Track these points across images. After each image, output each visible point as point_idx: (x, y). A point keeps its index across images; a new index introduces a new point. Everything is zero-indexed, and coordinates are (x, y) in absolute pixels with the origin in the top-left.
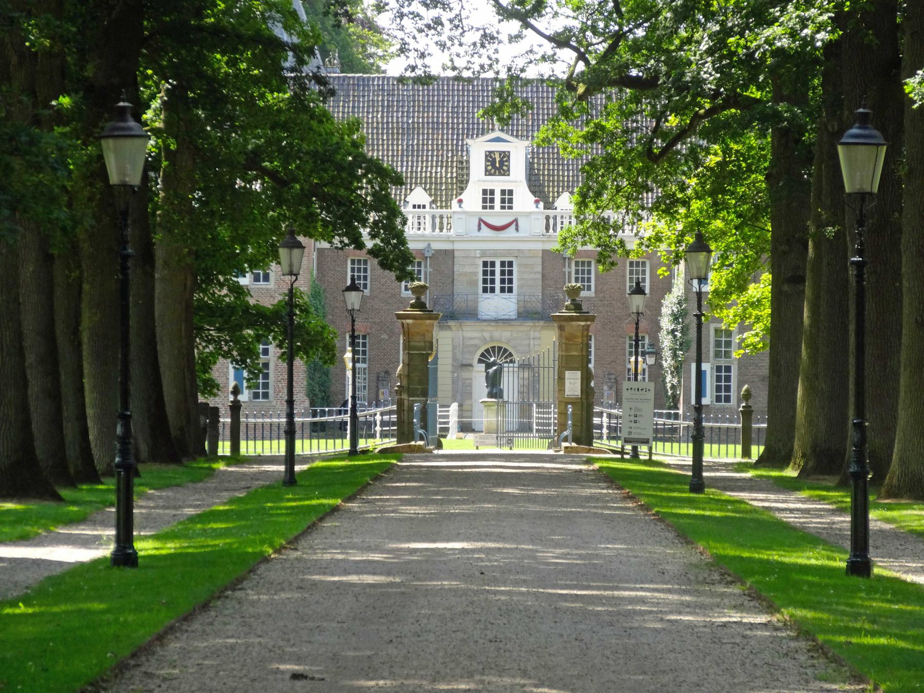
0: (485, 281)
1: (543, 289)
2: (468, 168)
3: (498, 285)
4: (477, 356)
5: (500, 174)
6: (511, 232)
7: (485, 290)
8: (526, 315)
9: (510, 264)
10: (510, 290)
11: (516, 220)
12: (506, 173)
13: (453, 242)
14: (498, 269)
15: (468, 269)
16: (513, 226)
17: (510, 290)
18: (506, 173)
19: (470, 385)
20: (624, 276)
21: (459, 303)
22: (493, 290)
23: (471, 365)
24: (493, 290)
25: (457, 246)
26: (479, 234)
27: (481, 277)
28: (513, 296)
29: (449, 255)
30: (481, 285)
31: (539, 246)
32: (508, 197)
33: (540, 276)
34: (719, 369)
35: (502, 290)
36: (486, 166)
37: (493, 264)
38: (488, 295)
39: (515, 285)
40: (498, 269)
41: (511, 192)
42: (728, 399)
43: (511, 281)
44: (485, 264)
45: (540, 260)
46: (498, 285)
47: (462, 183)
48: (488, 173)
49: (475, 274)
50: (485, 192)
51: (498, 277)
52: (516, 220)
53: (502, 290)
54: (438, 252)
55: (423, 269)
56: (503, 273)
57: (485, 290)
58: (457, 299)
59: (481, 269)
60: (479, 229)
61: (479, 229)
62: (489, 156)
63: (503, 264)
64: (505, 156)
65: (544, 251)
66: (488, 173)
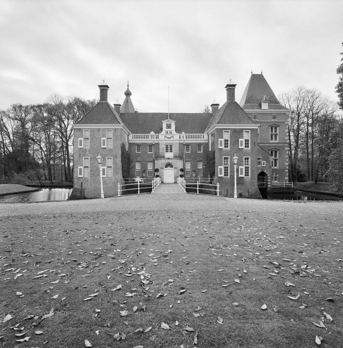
0: (166, 150)
1: (179, 151)
2: (163, 129)
3: (169, 150)
4: (165, 166)
5: (169, 128)
6: (172, 139)
7: (166, 152)
8: (175, 157)
9: (172, 146)
10: (172, 152)
11: (173, 136)
12: (171, 128)
13: (159, 141)
14: (169, 147)
15: (162, 147)
16: (172, 138)
17: (172, 152)
18: (171, 128)
19: (163, 173)
20: (197, 148)
21: (161, 154)
22: (168, 152)
23: (163, 168)
24: (168, 152)
25: (160, 142)
26: (165, 139)
27: (165, 149)
28: (173, 153)
29: (158, 144)
30: (165, 150)
31: (178, 142)
32: (171, 133)
33: (178, 148)
34: (225, 168)
35: (170, 152)
36: (166, 127)
37: (168, 146)
38: (167, 153)
39: (173, 151)
40: (169, 147)
41: (171, 132)
42: (227, 175)
43: (172, 150)
44: (166, 146)
45: (178, 145)
46: (169, 150)
47: (161, 130)
48: (167, 128)
49: (164, 148)
50: (166, 132)
51: (169, 149)
52: (173, 136)
53: (170, 152)
54: (156, 143)
55: (152, 147)
56: (170, 148)
57: (166, 152)
58: (160, 153)
59: (165, 147)
60: (165, 138)
61: (165, 138)
62: (167, 124)
63: (170, 146)
64: (171, 124)
65: (179, 143)
66: (167, 128)
